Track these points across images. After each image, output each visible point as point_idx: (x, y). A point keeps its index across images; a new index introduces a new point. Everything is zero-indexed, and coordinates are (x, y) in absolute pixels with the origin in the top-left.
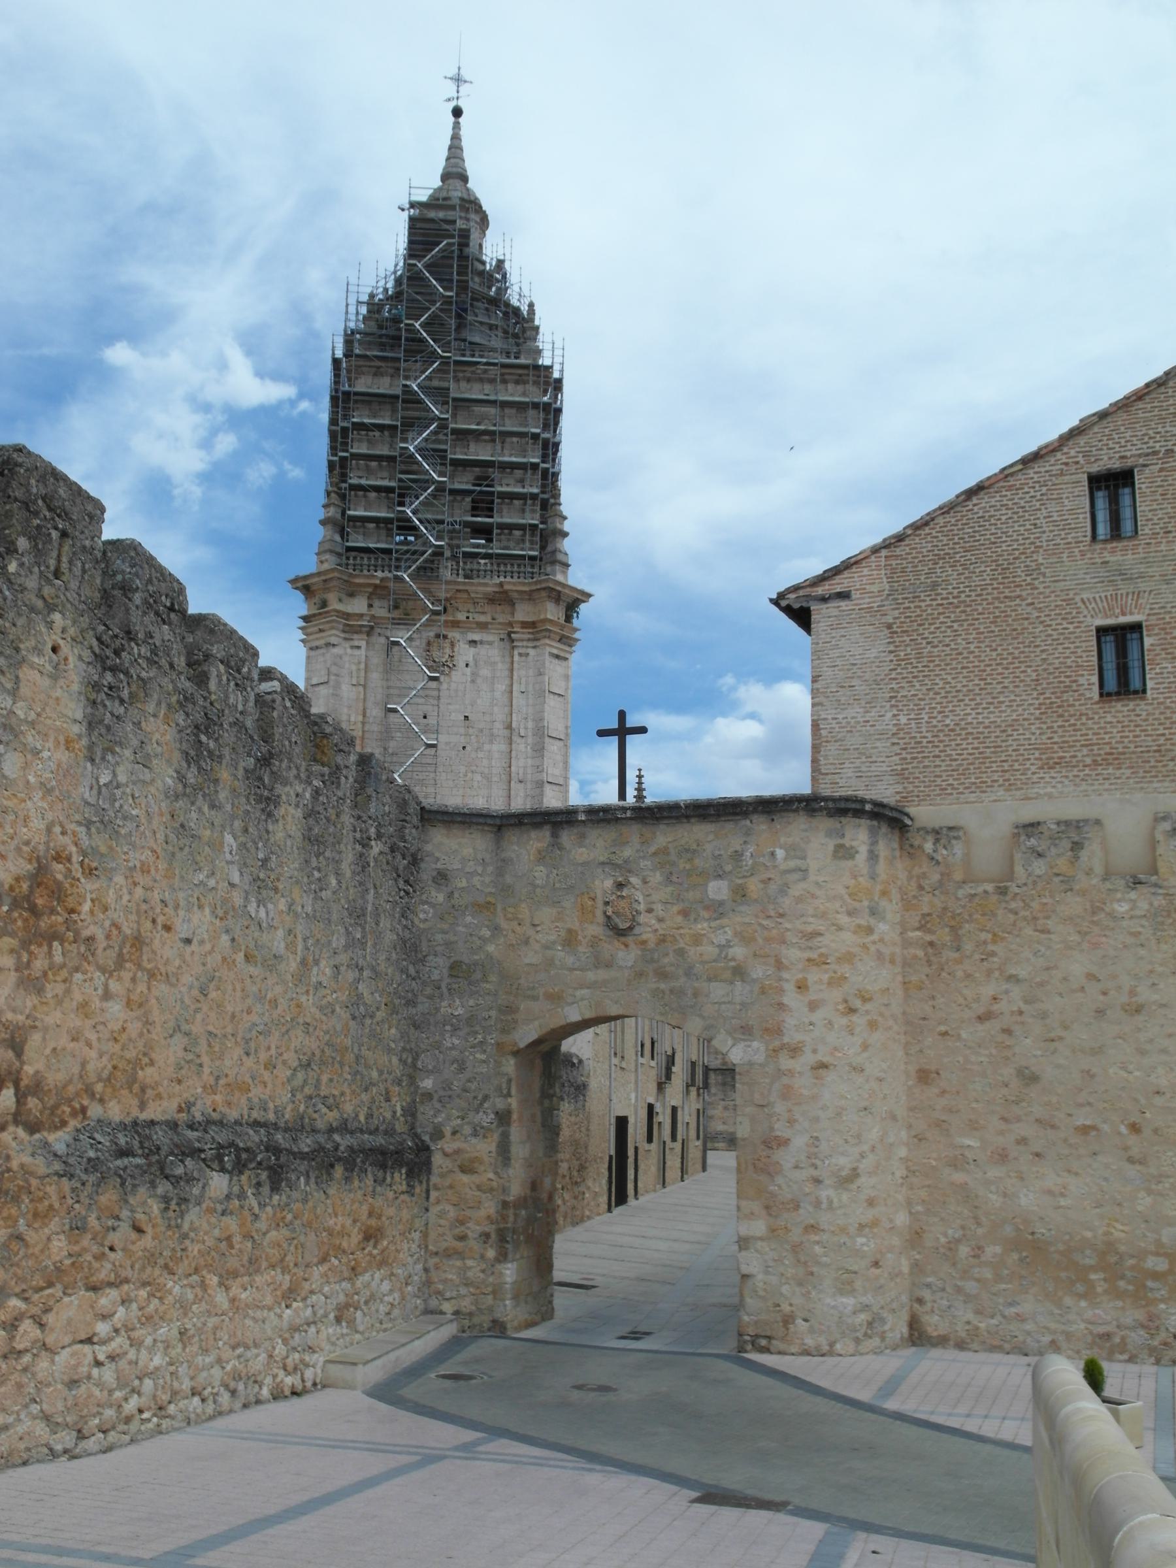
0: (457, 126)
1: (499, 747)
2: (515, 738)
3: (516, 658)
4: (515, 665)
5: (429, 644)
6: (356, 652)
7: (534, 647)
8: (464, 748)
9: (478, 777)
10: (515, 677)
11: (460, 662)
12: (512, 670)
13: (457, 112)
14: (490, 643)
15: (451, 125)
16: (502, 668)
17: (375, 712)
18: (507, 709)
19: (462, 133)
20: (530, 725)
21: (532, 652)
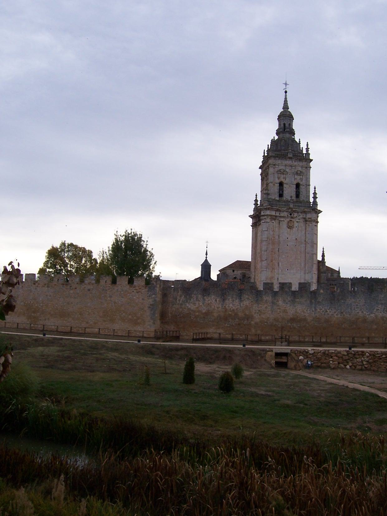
0: (286, 96)
1: (303, 245)
2: (307, 244)
3: (307, 226)
4: (307, 228)
5: (288, 222)
6: (273, 224)
7: (311, 223)
8: (296, 246)
9: (299, 252)
10: (307, 230)
11: (295, 226)
12: (306, 229)
13: (286, 92)
14: (301, 222)
15: (284, 95)
16: (304, 228)
17: (277, 237)
18: (305, 237)
19: (287, 97)
20: (310, 241)
21: (310, 224)
